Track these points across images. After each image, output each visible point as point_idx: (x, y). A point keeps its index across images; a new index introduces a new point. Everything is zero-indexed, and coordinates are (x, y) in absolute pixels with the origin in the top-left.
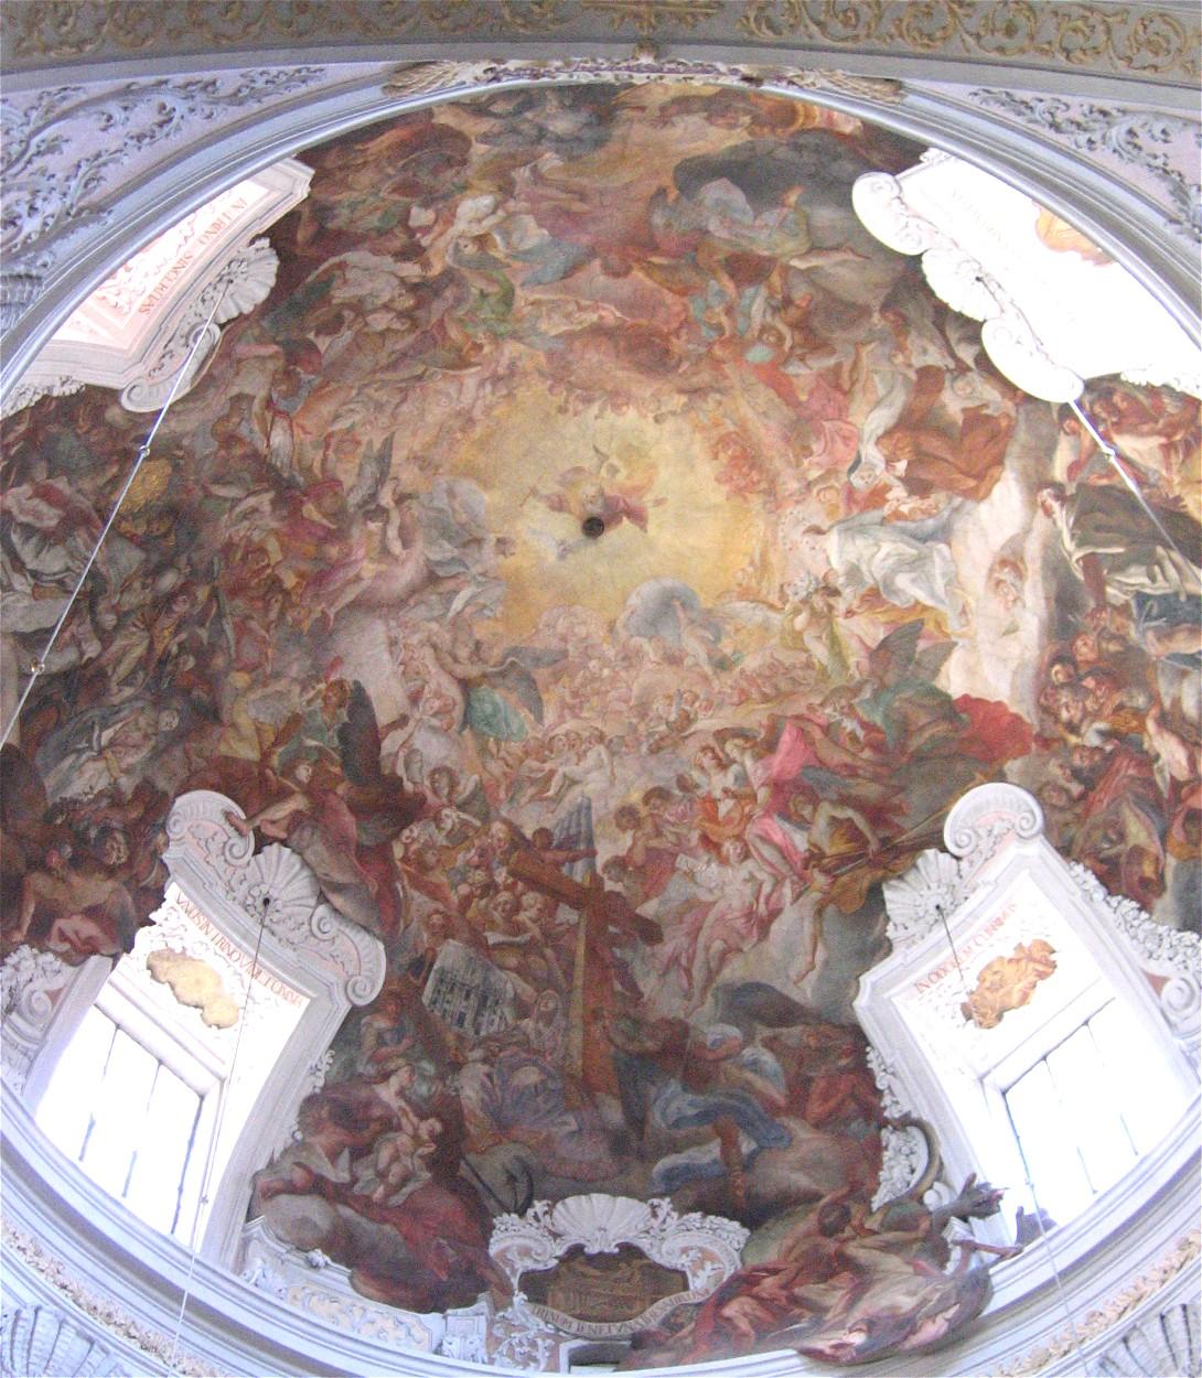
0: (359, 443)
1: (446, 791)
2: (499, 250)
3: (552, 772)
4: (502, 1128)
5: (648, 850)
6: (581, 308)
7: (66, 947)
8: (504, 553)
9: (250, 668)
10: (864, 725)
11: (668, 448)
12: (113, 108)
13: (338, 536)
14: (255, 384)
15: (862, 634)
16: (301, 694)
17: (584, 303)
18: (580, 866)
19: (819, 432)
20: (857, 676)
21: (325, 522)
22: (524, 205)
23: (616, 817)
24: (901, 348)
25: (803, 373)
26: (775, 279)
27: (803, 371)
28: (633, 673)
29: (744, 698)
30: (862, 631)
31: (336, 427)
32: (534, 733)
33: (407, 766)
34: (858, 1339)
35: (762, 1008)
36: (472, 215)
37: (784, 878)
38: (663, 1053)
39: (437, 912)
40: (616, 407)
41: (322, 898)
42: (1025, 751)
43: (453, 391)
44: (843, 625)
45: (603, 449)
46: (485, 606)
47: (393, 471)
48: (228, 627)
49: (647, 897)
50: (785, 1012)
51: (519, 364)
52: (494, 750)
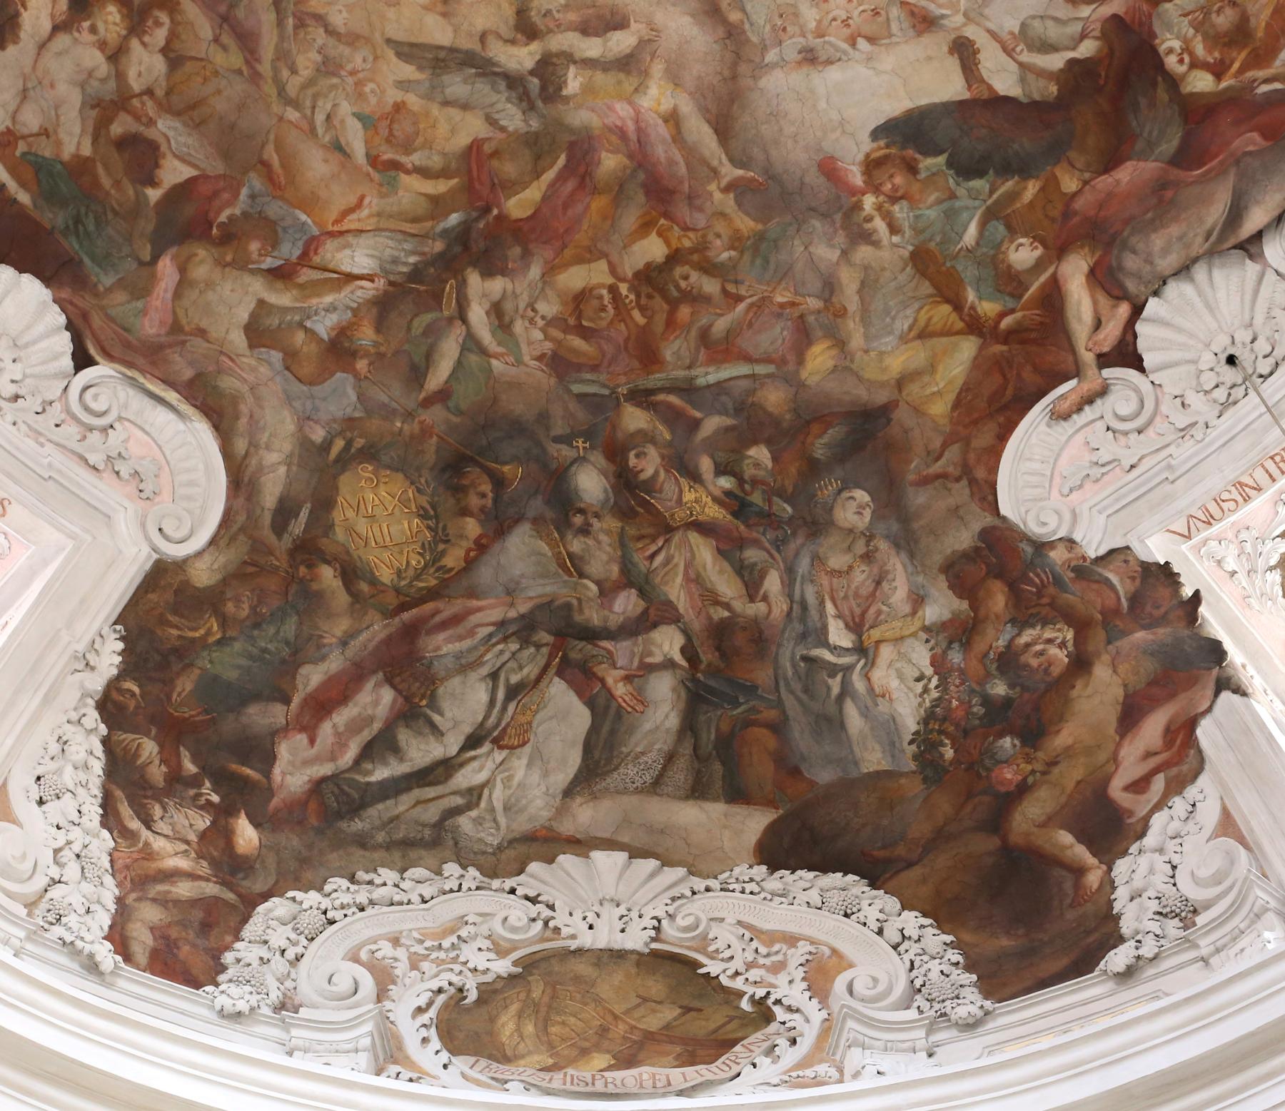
0: (399, 107)
7: (1159, 783)
9: (803, 336)
13: (581, 151)
14: (231, 299)
16: (876, 244)
21: (550, 175)
31: (358, 149)
33: (1047, 47)
41: (1251, 247)
47: (466, 44)
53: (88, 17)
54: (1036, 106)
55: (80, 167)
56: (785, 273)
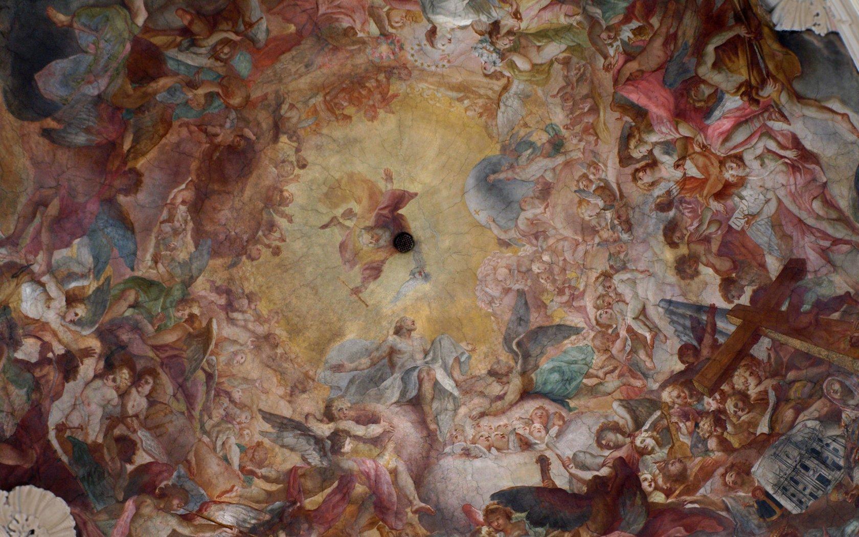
0: (259, 444)
1: (620, 437)
3: (630, 330)
5: (720, 254)
6: (170, 220)
8: (410, 331)
10: (627, 19)
11: (333, 160)
13: (346, 480)
15: (537, 7)
17: (165, 215)
18: (721, 324)
19: (330, 19)
20: (578, 18)
21: (328, 491)
22: (41, 257)
23: (683, 278)
26: (158, 40)
27: (264, 25)
28: (552, 232)
29: (591, 130)
32: (588, 339)
36: (40, 305)
37: (765, 125)
39: (724, 475)
40: (284, 201)
43: (233, 349)
44: (528, 24)
45: (326, 219)
46: (457, 359)
47: (297, 418)
49: (763, 266)
51: (219, 283)
52: (594, 381)
53: (113, 373)
54: (575, 496)
55: (96, 448)
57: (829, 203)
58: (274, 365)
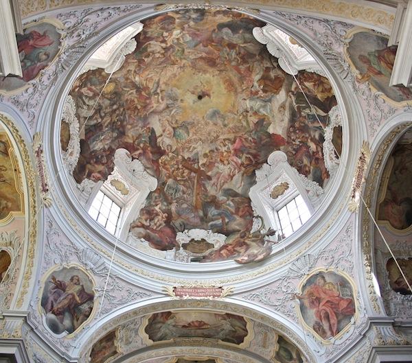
2: (181, 41)
4: (179, 216)
9: (131, 125)
12: (99, 13)
13: (149, 98)
14: (132, 68)
24: (262, 63)
25: (242, 68)
30: (253, 119)
31: (149, 76)
32: (187, 138)
34: (246, 258)
35: (230, 193)
38: (211, 202)
40: (205, 73)
42: (284, 145)
48: (127, 116)
50: (236, 195)
54: (156, 144)
56: (137, 121)
57: (224, 183)
58: (170, 78)
